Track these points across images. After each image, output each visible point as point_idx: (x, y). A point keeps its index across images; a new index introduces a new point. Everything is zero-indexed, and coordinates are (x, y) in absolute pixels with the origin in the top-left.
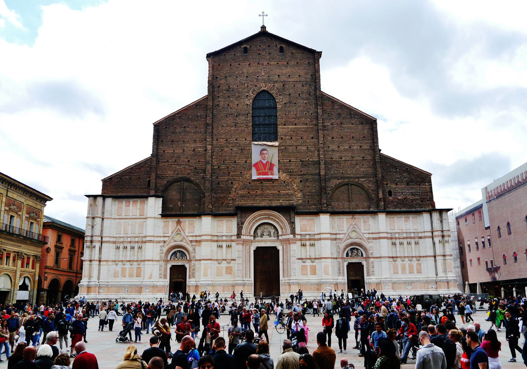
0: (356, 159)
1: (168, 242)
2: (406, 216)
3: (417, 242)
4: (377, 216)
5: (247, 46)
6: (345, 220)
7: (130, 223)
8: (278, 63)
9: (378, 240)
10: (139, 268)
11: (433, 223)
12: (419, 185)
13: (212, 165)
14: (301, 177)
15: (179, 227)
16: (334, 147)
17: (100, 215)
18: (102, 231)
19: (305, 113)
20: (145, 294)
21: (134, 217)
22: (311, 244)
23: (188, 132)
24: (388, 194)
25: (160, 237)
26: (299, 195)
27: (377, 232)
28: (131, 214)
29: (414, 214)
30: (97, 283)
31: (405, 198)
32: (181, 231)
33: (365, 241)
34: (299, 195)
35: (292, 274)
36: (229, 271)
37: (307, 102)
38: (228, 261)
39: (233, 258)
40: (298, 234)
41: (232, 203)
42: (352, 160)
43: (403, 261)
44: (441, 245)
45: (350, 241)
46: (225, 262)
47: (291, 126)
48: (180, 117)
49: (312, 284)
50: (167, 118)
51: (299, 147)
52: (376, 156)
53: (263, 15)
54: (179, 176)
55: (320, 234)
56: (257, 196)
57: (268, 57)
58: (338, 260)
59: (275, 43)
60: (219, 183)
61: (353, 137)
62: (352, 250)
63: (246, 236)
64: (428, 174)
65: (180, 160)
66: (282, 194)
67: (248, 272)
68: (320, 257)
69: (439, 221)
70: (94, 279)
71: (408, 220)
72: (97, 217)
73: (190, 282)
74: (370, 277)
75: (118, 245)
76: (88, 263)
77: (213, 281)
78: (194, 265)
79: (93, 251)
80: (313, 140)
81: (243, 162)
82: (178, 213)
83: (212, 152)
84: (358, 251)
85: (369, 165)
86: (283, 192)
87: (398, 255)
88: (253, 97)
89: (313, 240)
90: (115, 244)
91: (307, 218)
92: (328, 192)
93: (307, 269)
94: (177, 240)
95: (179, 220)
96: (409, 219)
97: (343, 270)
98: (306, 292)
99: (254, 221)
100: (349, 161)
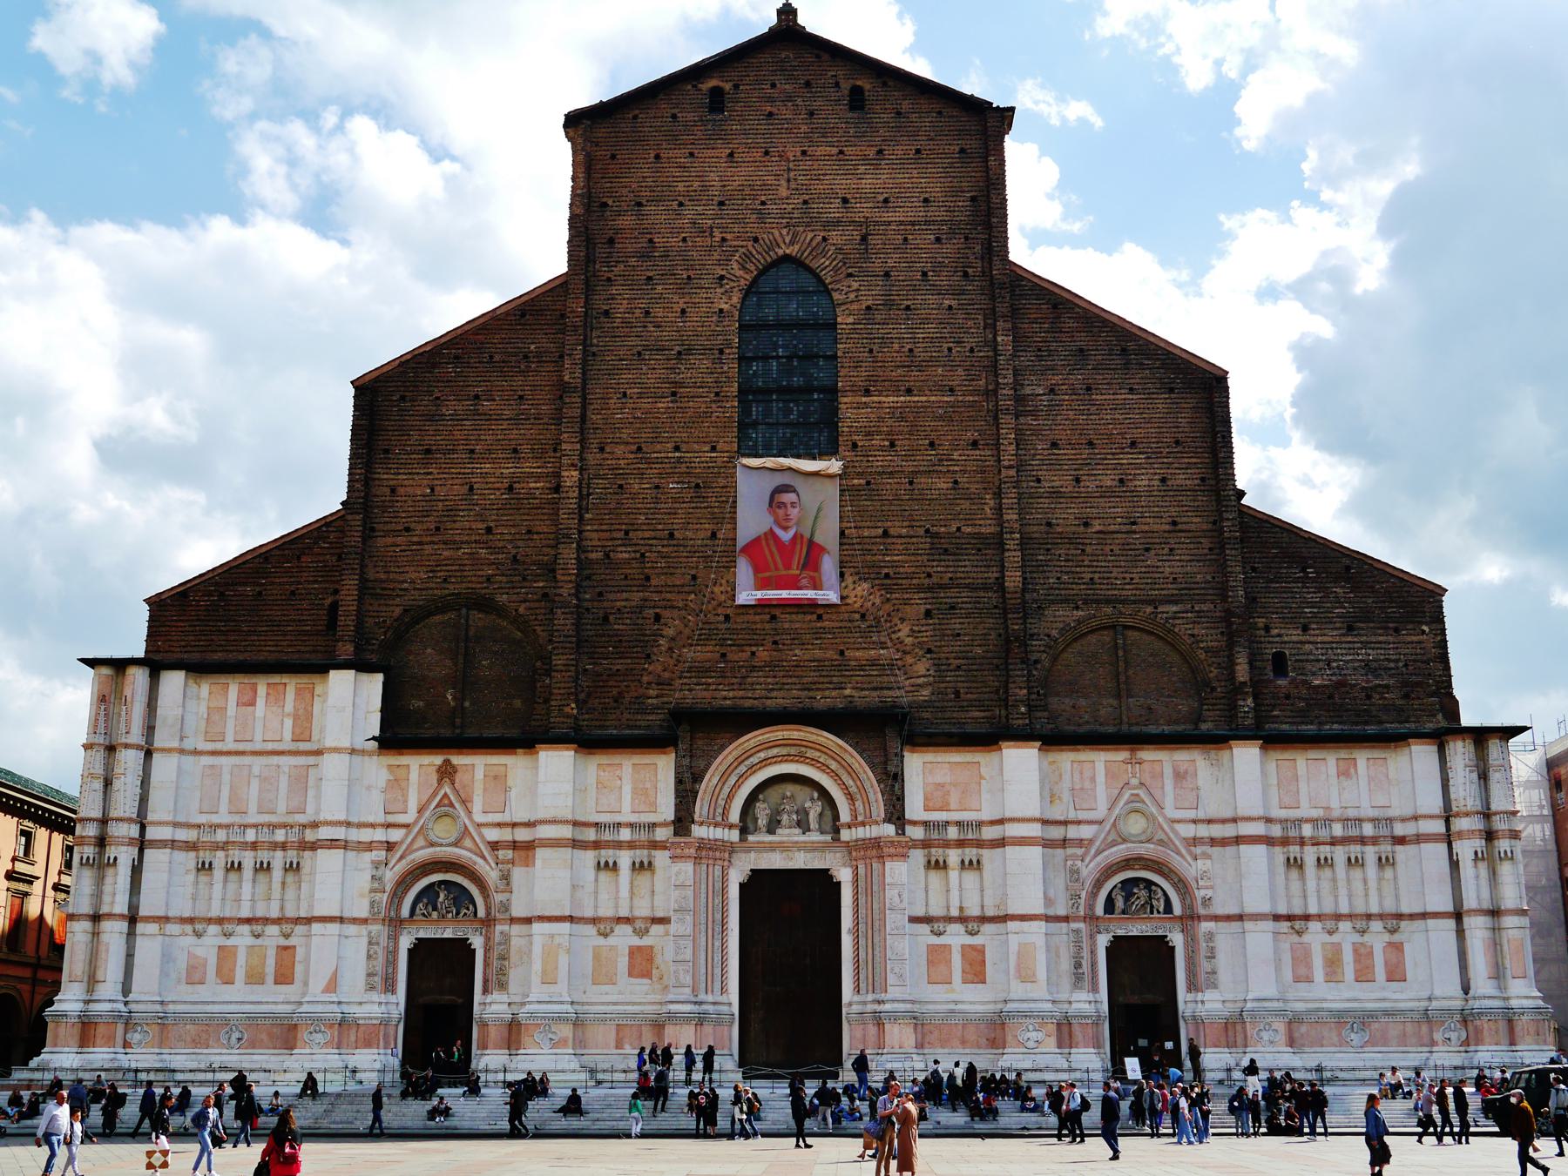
0: (1146, 528)
1: (404, 847)
2: (1343, 754)
3: (1387, 858)
4: (1225, 754)
5: (721, 84)
7: (256, 771)
8: (841, 152)
10: (286, 948)
11: (1451, 783)
12: (1396, 630)
13: (581, 549)
14: (929, 595)
15: (447, 789)
16: (1058, 480)
17: (136, 736)
18: (143, 800)
20: (308, 1051)
21: (270, 746)
22: (967, 863)
23: (489, 418)
24: (1270, 668)
25: (373, 826)
26: (921, 668)
27: (1228, 814)
28: (258, 737)
29: (1373, 747)
30: (121, 1007)
31: (1341, 684)
32: (457, 805)
33: (1179, 853)
35: (891, 979)
36: (642, 964)
37: (953, 303)
38: (639, 924)
39: (660, 914)
40: (914, 823)
41: (657, 697)
42: (1128, 532)
43: (1330, 933)
44: (1483, 866)
45: (1119, 852)
46: (628, 929)
47: (891, 399)
48: (456, 357)
49: (967, 1021)
50: (408, 361)
51: (922, 480)
52: (1225, 515)
54: (451, 587)
55: (1001, 822)
56: (754, 668)
57: (804, 128)
58: (1074, 925)
60: (606, 619)
61: (1133, 444)
63: (712, 828)
64: (1431, 587)
65: (457, 525)
66: (853, 663)
67: (718, 971)
68: (1001, 914)
69: (1475, 775)
70: (109, 988)
71: (1352, 770)
72: (127, 746)
73: (489, 1006)
74: (1200, 996)
75: (206, 856)
76: (86, 925)
77: (578, 1003)
78: (507, 938)
79: (109, 880)
80: (978, 452)
81: (701, 534)
82: (446, 732)
84: (1150, 891)
86: (859, 654)
87: (1313, 910)
88: (743, 282)
89: (971, 846)
90: (192, 854)
91: (952, 760)
92: (1034, 657)
94: (444, 842)
95: (447, 762)
96: (1355, 765)
97: (1094, 964)
98: (946, 1051)
99: (743, 768)
100: (1119, 535)
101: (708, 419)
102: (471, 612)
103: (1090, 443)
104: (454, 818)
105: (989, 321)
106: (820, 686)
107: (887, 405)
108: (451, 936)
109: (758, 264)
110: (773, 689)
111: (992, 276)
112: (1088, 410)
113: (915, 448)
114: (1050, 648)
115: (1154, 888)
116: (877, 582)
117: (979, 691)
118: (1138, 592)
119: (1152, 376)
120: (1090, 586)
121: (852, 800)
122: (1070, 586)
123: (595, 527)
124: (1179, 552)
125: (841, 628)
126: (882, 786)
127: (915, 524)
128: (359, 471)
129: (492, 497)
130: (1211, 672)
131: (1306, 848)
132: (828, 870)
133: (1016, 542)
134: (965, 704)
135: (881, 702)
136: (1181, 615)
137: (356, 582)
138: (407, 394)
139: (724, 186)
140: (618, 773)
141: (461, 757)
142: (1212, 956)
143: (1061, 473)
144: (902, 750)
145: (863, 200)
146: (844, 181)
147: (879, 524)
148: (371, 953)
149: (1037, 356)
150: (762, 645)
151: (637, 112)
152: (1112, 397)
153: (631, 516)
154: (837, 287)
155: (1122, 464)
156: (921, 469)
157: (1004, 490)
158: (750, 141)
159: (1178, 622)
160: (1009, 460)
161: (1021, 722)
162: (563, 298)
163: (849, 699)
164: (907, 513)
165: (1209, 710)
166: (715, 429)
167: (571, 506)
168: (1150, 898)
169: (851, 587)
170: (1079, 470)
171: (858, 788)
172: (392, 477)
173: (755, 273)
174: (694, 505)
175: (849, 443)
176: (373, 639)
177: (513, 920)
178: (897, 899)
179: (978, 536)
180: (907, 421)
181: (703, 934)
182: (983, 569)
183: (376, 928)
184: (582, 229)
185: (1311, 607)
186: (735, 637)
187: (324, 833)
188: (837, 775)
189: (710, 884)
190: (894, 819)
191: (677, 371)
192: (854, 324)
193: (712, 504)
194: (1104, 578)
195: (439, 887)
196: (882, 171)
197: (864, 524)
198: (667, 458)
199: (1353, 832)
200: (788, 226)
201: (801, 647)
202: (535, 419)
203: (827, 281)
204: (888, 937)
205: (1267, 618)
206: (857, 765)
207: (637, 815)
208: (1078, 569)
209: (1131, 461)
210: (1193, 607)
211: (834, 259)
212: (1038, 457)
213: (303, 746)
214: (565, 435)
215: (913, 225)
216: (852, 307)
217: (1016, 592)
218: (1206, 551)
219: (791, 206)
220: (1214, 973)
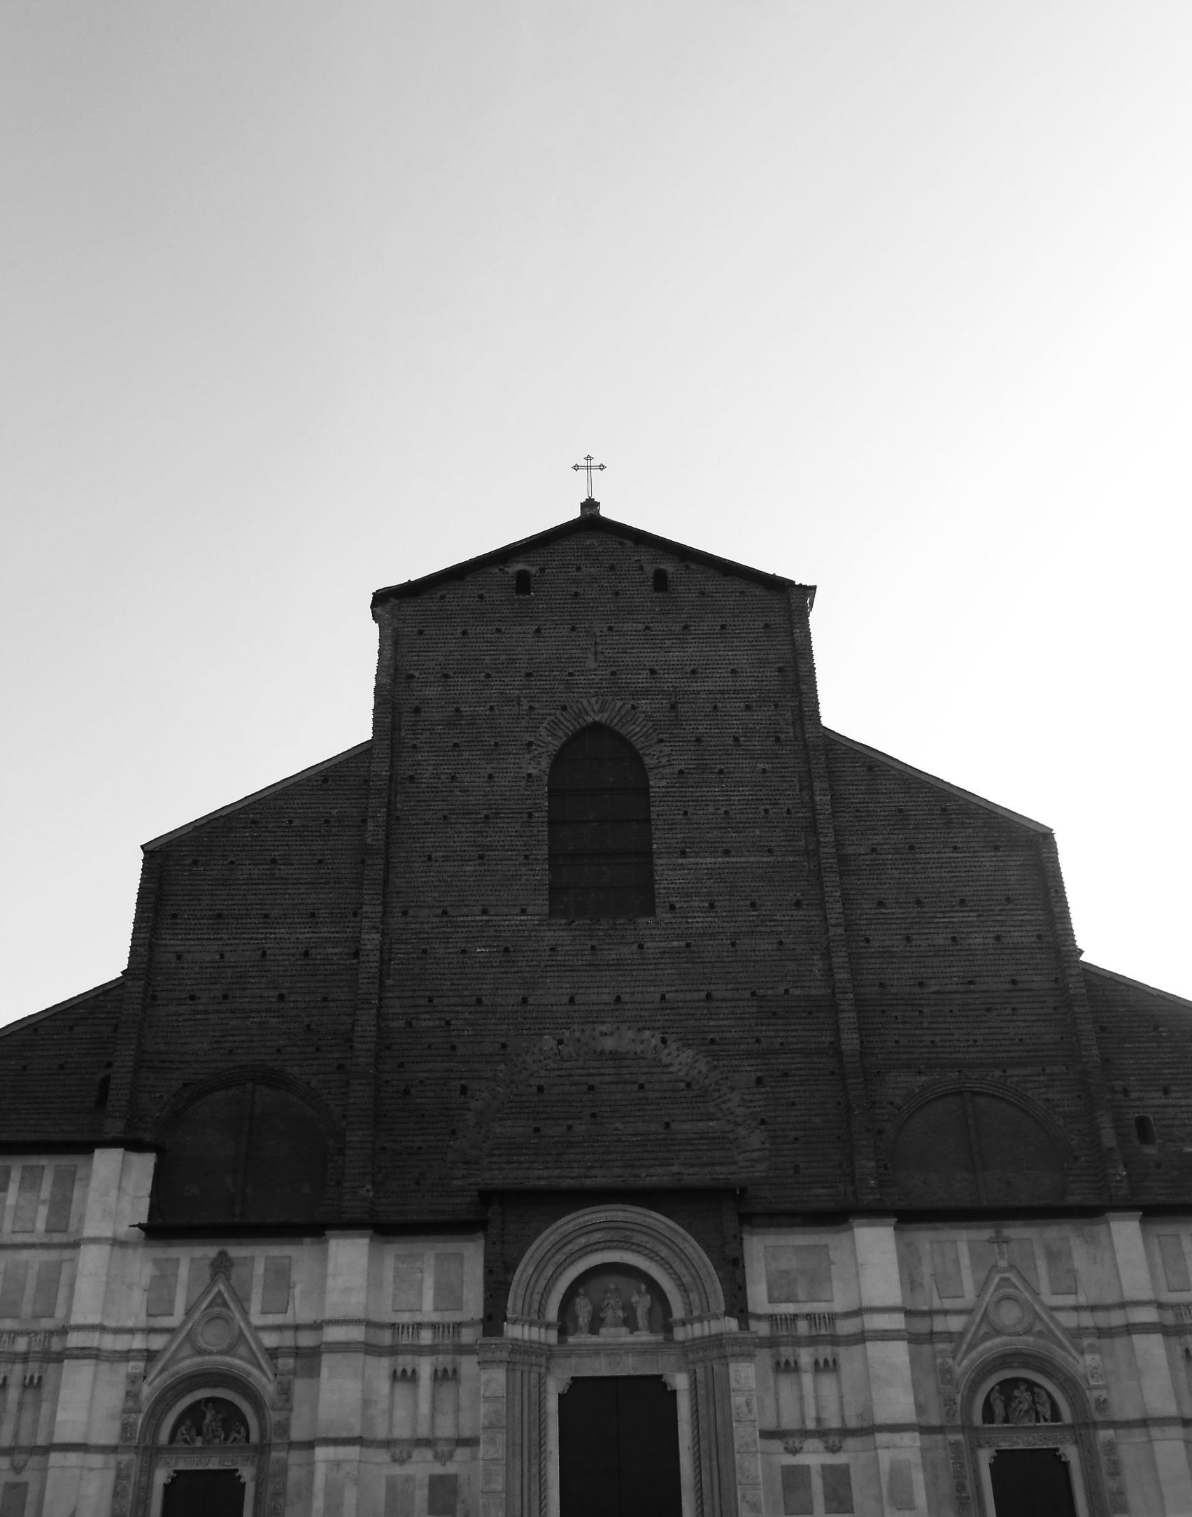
0: (985, 987)
1: (167, 1356)
4: (1100, 1229)
5: (527, 568)
6: (964, 1249)
8: (647, 628)
9: (1119, 1342)
10: (15, 1486)
13: (379, 1015)
15: (221, 1287)
21: (20, 1238)
22: (821, 1362)
25: (131, 1331)
26: (756, 1139)
32: (232, 1305)
34: (756, 1139)
37: (766, 766)
38: (442, 1448)
39: (467, 1433)
40: (759, 1317)
41: (463, 1177)
42: (967, 992)
45: (995, 1344)
46: (428, 1454)
47: (708, 860)
48: (254, 822)
50: (203, 825)
53: (589, 466)
58: (952, 1437)
60: (407, 1092)
61: (962, 902)
62: (1007, 1386)
68: (865, 1425)
78: (284, 1469)
80: (802, 912)
83: (382, 962)
84: (1033, 1394)
85: (1039, 1011)
86: (686, 1126)
88: (551, 748)
93: (808, 1486)
94: (214, 1349)
95: (223, 1254)
97: (978, 1487)
99: (560, 1257)
100: (958, 996)
101: (519, 882)
103: (918, 902)
104: (228, 1320)
105: (805, 784)
106: (645, 1162)
108: (216, 1468)
109: (567, 731)
110: (592, 1167)
111: (805, 740)
112: (913, 868)
113: (736, 908)
115: (1036, 1389)
116: (704, 1048)
118: (983, 1055)
119: (975, 835)
121: (686, 1291)
123: (396, 994)
124: (1023, 1012)
127: (738, 986)
128: (143, 935)
129: (287, 963)
130: (1072, 1139)
132: (661, 1376)
135: (713, 1179)
137: (133, 1053)
138: (200, 858)
139: (532, 659)
140: (418, 1264)
141: (238, 1248)
142: (1115, 1471)
143: (891, 932)
144: (741, 1232)
145: (671, 672)
146: (652, 654)
148: (119, 1488)
149: (857, 816)
150: (579, 1118)
151: (444, 592)
152: (936, 856)
154: (648, 752)
155: (953, 922)
157: (833, 949)
158: (556, 618)
159: (1030, 1085)
160: (837, 918)
161: (870, 1197)
162: (367, 764)
164: (731, 976)
166: (525, 892)
167: (371, 970)
168: (1034, 1403)
169: (675, 1054)
170: (909, 929)
171: (692, 1276)
172: (178, 942)
173: (565, 739)
174: (503, 970)
175: (667, 905)
177: (292, 1445)
178: (745, 1409)
180: (726, 882)
181: (518, 1457)
182: (815, 1033)
183: (125, 1458)
184: (389, 697)
185: (1170, 1068)
186: (549, 1109)
187: (75, 1340)
188: (668, 1263)
189: (526, 1393)
191: (484, 834)
192: (667, 787)
193: (523, 969)
194: (946, 1041)
195: (206, 1405)
196: (688, 645)
197: (685, 987)
198: (474, 921)
200: (596, 694)
202: (335, 883)
203: (638, 747)
204: (737, 1456)
206: (691, 1250)
207: (439, 1314)
208: (917, 1032)
209: (961, 919)
210: (1044, 1070)
211: (644, 726)
212: (865, 917)
213: (57, 1238)
214: (366, 897)
215: (723, 694)
216: (664, 772)
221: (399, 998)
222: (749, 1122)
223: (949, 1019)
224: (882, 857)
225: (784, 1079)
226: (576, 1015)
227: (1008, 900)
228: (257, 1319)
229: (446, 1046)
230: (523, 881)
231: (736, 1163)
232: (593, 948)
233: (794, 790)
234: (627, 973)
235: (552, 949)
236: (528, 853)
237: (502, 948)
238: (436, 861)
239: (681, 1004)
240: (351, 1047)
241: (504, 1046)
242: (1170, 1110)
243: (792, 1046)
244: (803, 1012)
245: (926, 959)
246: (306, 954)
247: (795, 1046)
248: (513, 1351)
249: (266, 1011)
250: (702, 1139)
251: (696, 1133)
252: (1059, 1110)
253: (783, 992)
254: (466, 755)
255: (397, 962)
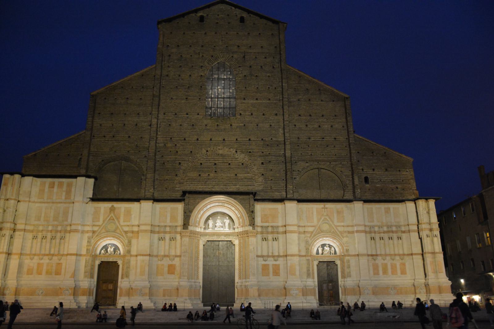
0: (327, 140)
1: (98, 232)
6: (315, 210)
10: (59, 264)
12: (399, 171)
13: (156, 142)
14: (263, 158)
15: (112, 215)
19: (267, 87)
21: (58, 201)
32: (115, 220)
34: (261, 179)
37: (270, 75)
40: (258, 226)
47: (251, 101)
58: (307, 258)
59: (235, 13)
60: (164, 163)
61: (323, 116)
80: (277, 117)
84: (330, 247)
86: (241, 175)
87: (379, 253)
90: (32, 234)
95: (113, 206)
100: (319, 142)
101: (197, 106)
102: (123, 161)
103: (310, 115)
104: (115, 223)
106: (229, 185)
107: (250, 103)
112: (310, 106)
114: (299, 174)
115: (331, 247)
116: (247, 154)
117: (278, 186)
120: (311, 156)
122: (305, 156)
124: (337, 147)
125: (236, 167)
126: (248, 215)
127: (259, 137)
129: (131, 127)
130: (347, 182)
131: (376, 234)
133: (289, 142)
134: (274, 190)
136: (338, 165)
139: (203, 41)
147: (248, 137)
150: (212, 172)
151: (178, 21)
152: (316, 102)
153: (173, 133)
155: (319, 121)
156: (260, 121)
159: (337, 167)
160: (287, 119)
163: (239, 189)
165: (346, 193)
175: (239, 113)
176: (92, 169)
178: (253, 250)
179: (277, 141)
183: (88, 257)
185: (376, 164)
190: (252, 225)
191: (188, 92)
194: (315, 154)
198: (184, 117)
199: (390, 229)
200: (222, 52)
201: (223, 173)
202: (145, 105)
205: (362, 166)
208: (307, 151)
209: (322, 121)
210: (341, 163)
212: (295, 119)
217: (289, 157)
218: (344, 147)
219: (223, 47)
220: (350, 272)
221: (162, 138)
222: (259, 175)
223: (316, 148)
224: (300, 102)
225: (270, 163)
226: (212, 144)
227: (335, 116)
228: (122, 223)
229: (175, 151)
230: (198, 106)
231: (254, 185)
232: (218, 125)
233: (277, 82)
234: (227, 132)
235: (206, 125)
236: (200, 98)
237: (191, 125)
238: (174, 99)
239: (242, 142)
240: (149, 151)
241: (191, 152)
242: (374, 175)
243: (272, 154)
244: (276, 145)
245: (311, 131)
246: (136, 125)
247: (273, 154)
248: (191, 233)
249: (125, 140)
250: (246, 179)
251: (244, 177)
252: (344, 174)
253: (270, 139)
254: (183, 69)
255: (162, 127)
